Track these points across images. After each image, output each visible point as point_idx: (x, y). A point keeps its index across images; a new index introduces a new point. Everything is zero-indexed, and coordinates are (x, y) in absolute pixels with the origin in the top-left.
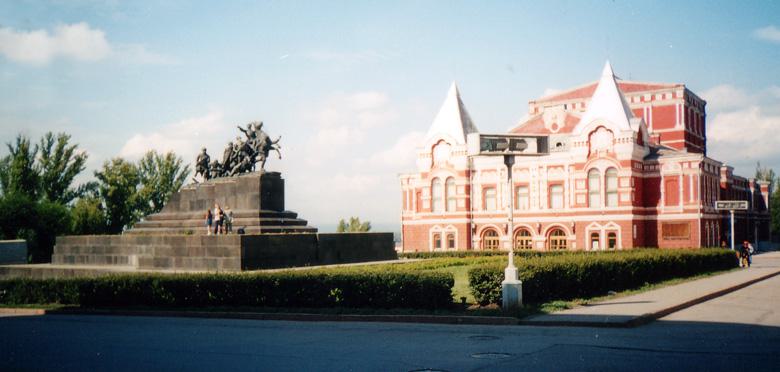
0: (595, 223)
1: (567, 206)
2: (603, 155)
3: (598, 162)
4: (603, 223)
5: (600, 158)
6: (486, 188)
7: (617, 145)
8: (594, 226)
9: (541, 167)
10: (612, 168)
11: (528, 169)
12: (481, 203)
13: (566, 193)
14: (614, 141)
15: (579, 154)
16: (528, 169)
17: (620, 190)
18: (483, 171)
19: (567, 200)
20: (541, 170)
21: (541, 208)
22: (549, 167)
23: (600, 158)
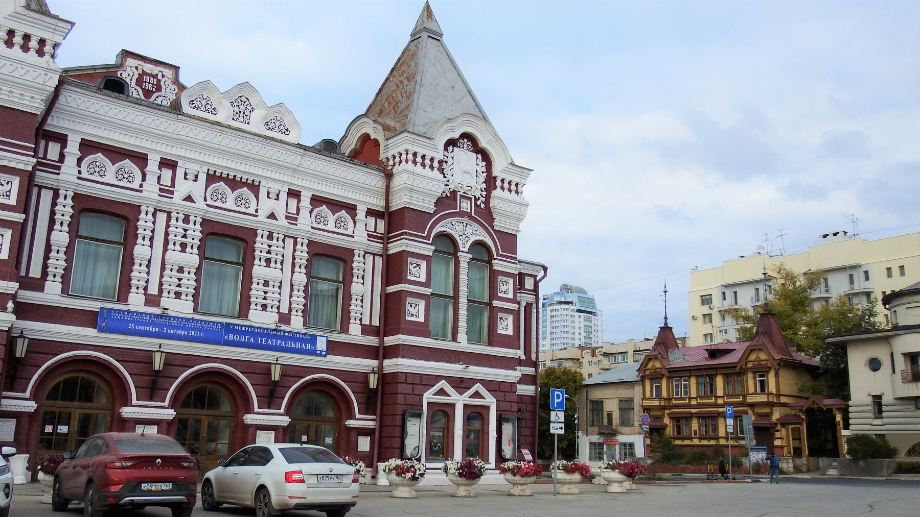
0: (443, 384)
1: (355, 328)
2: (466, 206)
3: (454, 220)
4: (461, 384)
5: (462, 214)
6: (86, 206)
7: (497, 193)
8: (442, 392)
9: (294, 194)
10: (479, 245)
11: (254, 188)
12: (58, 263)
13: (356, 288)
14: (490, 182)
15: (416, 188)
16: (254, 188)
17: (496, 303)
18: (88, 147)
19: (354, 307)
20: (293, 202)
21: (285, 319)
22: (317, 201)
23: (462, 214)
